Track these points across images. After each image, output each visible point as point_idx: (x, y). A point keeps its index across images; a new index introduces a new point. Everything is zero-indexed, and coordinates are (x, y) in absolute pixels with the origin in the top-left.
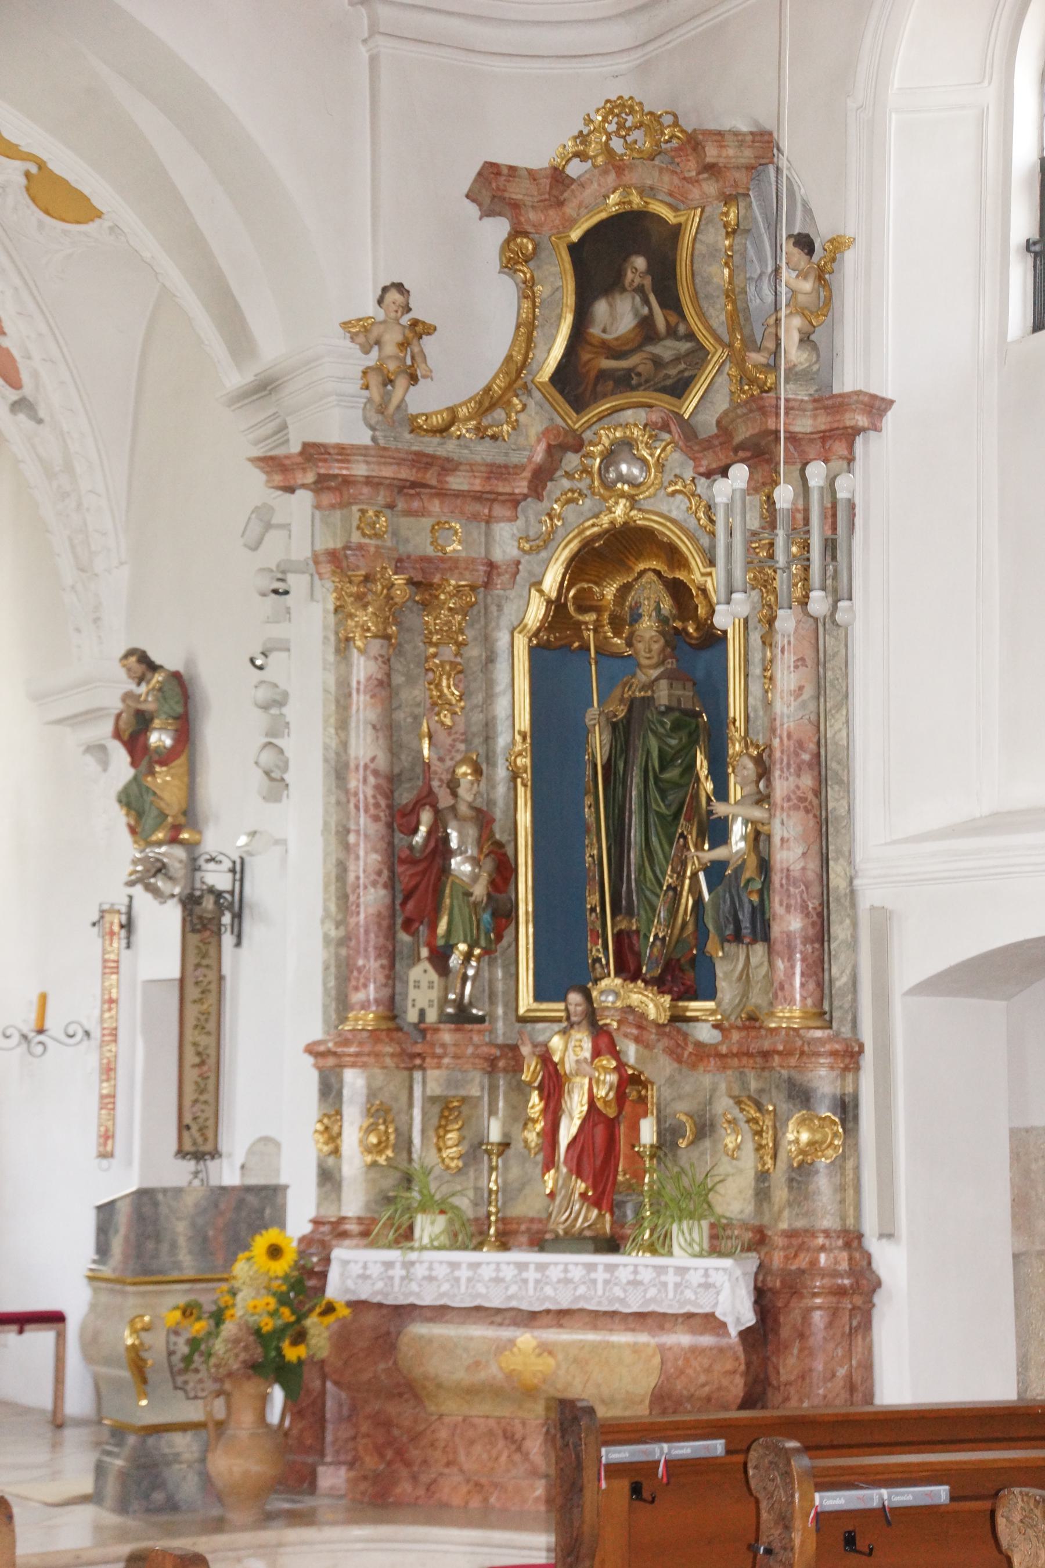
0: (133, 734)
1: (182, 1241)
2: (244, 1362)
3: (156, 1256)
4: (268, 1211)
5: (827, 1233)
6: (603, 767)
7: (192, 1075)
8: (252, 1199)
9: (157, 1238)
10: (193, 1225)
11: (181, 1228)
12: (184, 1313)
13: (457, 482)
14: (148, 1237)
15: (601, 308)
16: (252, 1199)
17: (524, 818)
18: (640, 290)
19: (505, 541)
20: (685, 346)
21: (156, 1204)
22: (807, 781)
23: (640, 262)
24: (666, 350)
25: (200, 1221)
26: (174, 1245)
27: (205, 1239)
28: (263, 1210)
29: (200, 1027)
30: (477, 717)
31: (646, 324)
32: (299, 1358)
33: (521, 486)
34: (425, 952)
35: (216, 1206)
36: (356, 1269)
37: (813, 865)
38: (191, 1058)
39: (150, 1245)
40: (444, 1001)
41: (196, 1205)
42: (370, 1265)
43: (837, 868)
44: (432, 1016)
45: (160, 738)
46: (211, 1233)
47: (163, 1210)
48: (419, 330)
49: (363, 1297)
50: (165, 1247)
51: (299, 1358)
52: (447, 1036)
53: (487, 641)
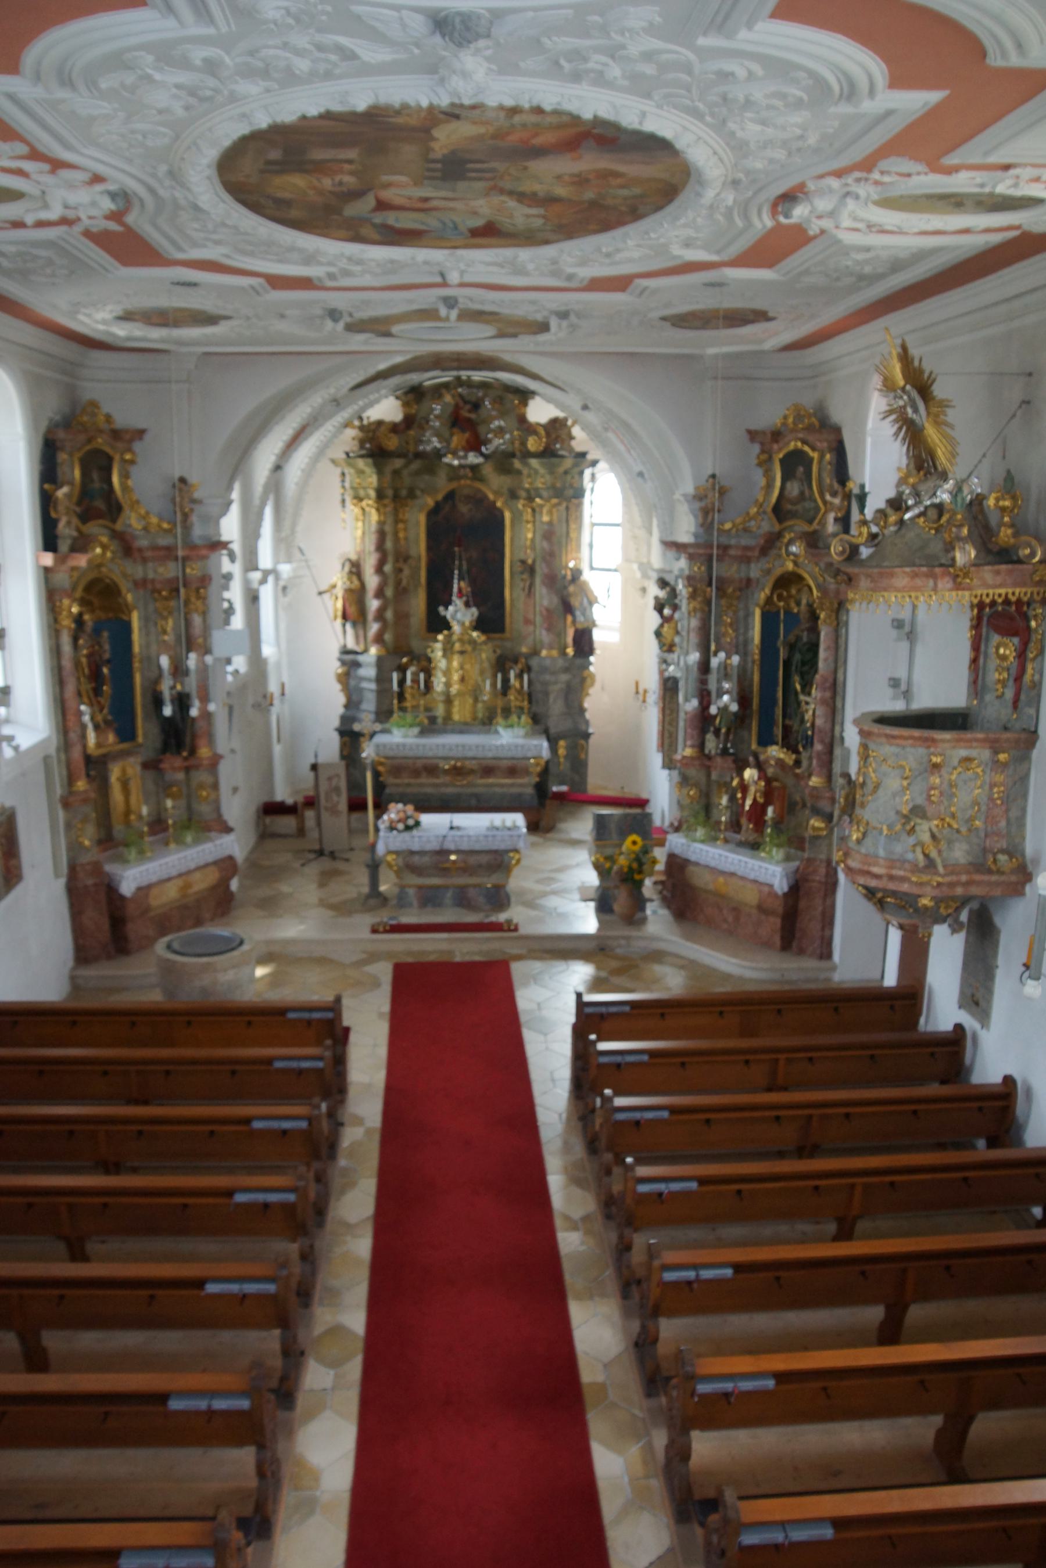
0: (659, 607)
5: (821, 861)
6: (784, 662)
7: (667, 741)
13: (732, 552)
15: (789, 485)
17: (756, 678)
18: (801, 480)
19: (754, 571)
20: (813, 505)
22: (828, 694)
23: (801, 469)
24: (807, 504)
29: (670, 724)
30: (741, 638)
31: (802, 493)
33: (756, 553)
34: (712, 729)
37: (828, 726)
38: (666, 735)
40: (717, 748)
43: (837, 729)
44: (713, 752)
45: (667, 611)
48: (723, 492)
52: (719, 760)
53: (747, 608)
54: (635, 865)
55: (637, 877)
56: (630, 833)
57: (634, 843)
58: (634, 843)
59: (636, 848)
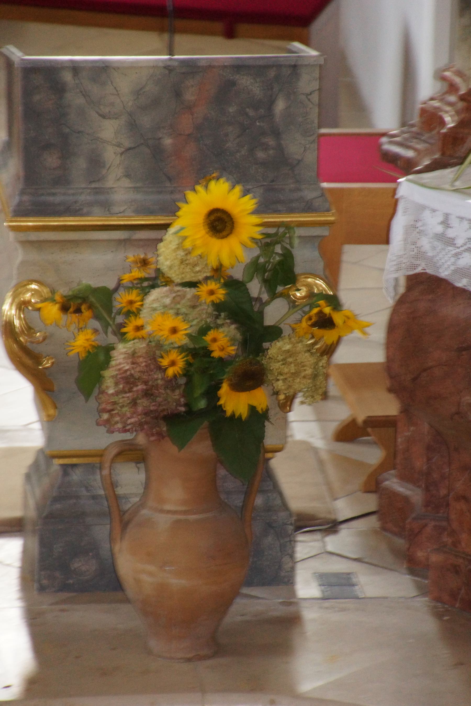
1: (111, 155)
2: (146, 413)
3: (62, 180)
4: (280, 105)
8: (245, 81)
9: (65, 148)
10: (133, 126)
11: (109, 130)
12: (65, 309)
14: (47, 147)
16: (245, 81)
21: (59, 89)
25: (146, 121)
26: (96, 163)
27: (157, 152)
28: (271, 103)
32: (252, 409)
35: (178, 94)
36: (433, 224)
39: (51, 160)
41: (138, 92)
42: (454, 222)
46: (168, 142)
47: (74, 99)
49: (444, 273)
50: (81, 163)
51: (252, 409)
54: (224, 341)
55: (235, 403)
56: (202, 176)
57: (220, 223)
58: (220, 223)
59: (234, 252)
